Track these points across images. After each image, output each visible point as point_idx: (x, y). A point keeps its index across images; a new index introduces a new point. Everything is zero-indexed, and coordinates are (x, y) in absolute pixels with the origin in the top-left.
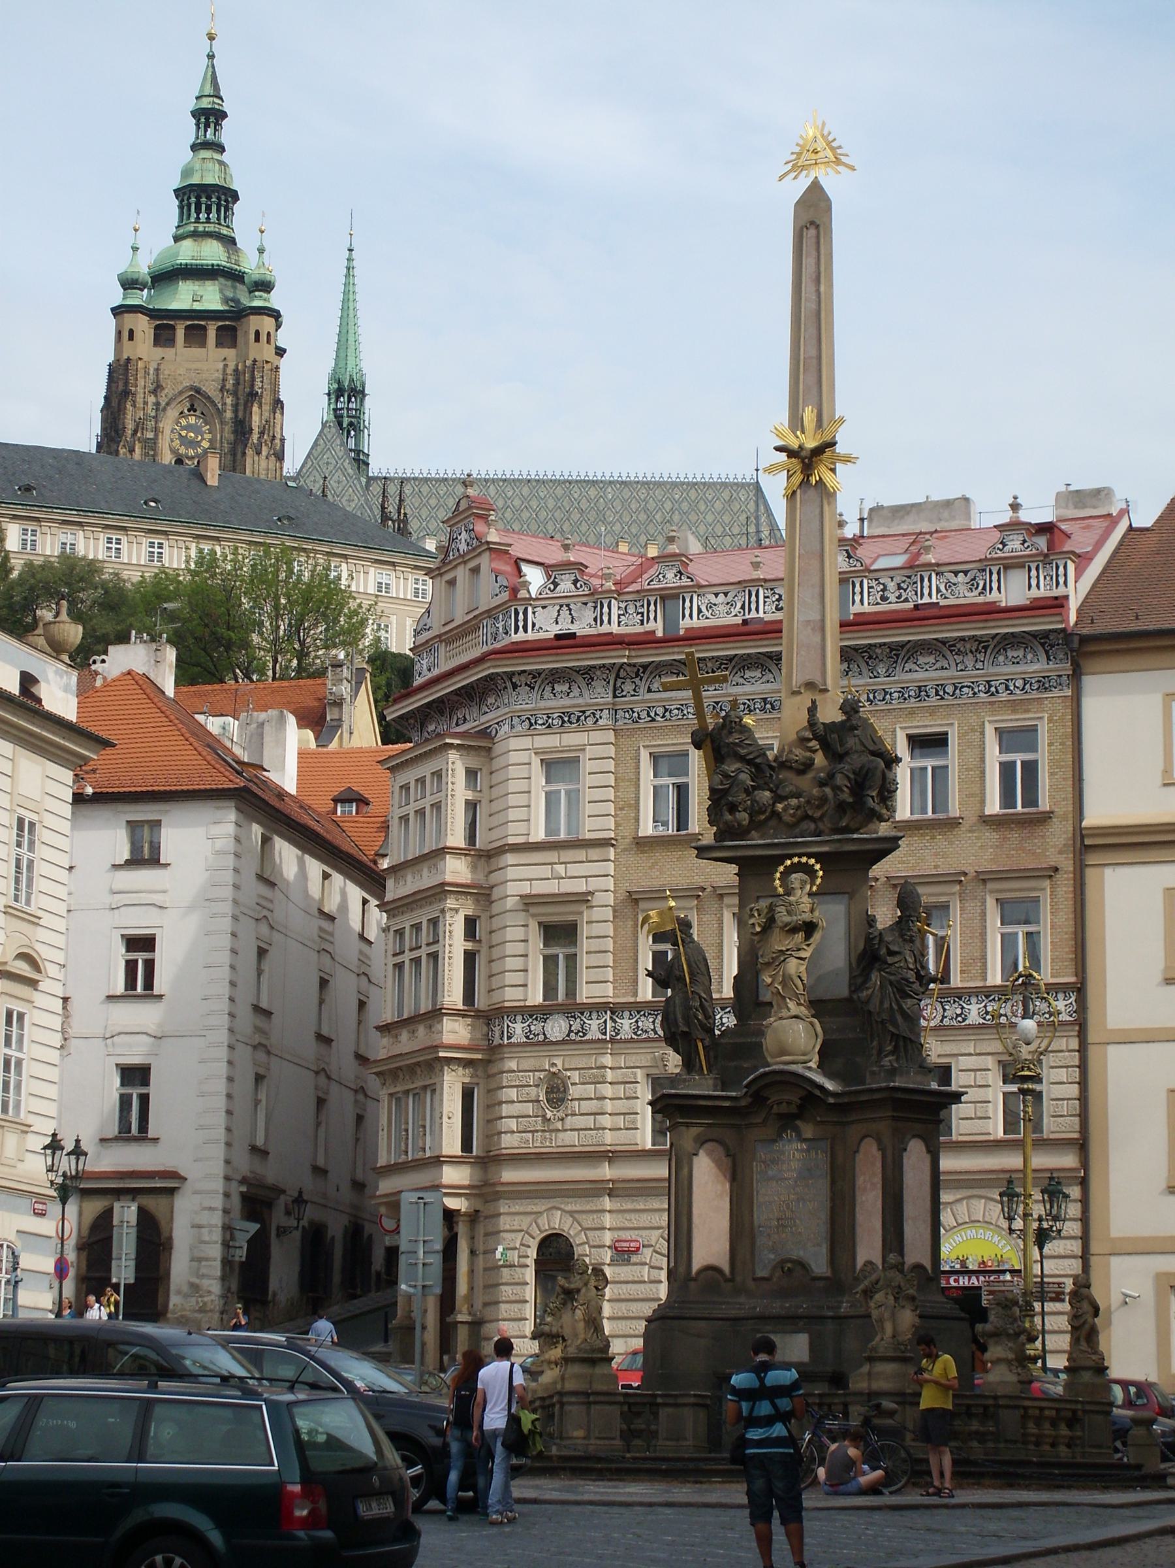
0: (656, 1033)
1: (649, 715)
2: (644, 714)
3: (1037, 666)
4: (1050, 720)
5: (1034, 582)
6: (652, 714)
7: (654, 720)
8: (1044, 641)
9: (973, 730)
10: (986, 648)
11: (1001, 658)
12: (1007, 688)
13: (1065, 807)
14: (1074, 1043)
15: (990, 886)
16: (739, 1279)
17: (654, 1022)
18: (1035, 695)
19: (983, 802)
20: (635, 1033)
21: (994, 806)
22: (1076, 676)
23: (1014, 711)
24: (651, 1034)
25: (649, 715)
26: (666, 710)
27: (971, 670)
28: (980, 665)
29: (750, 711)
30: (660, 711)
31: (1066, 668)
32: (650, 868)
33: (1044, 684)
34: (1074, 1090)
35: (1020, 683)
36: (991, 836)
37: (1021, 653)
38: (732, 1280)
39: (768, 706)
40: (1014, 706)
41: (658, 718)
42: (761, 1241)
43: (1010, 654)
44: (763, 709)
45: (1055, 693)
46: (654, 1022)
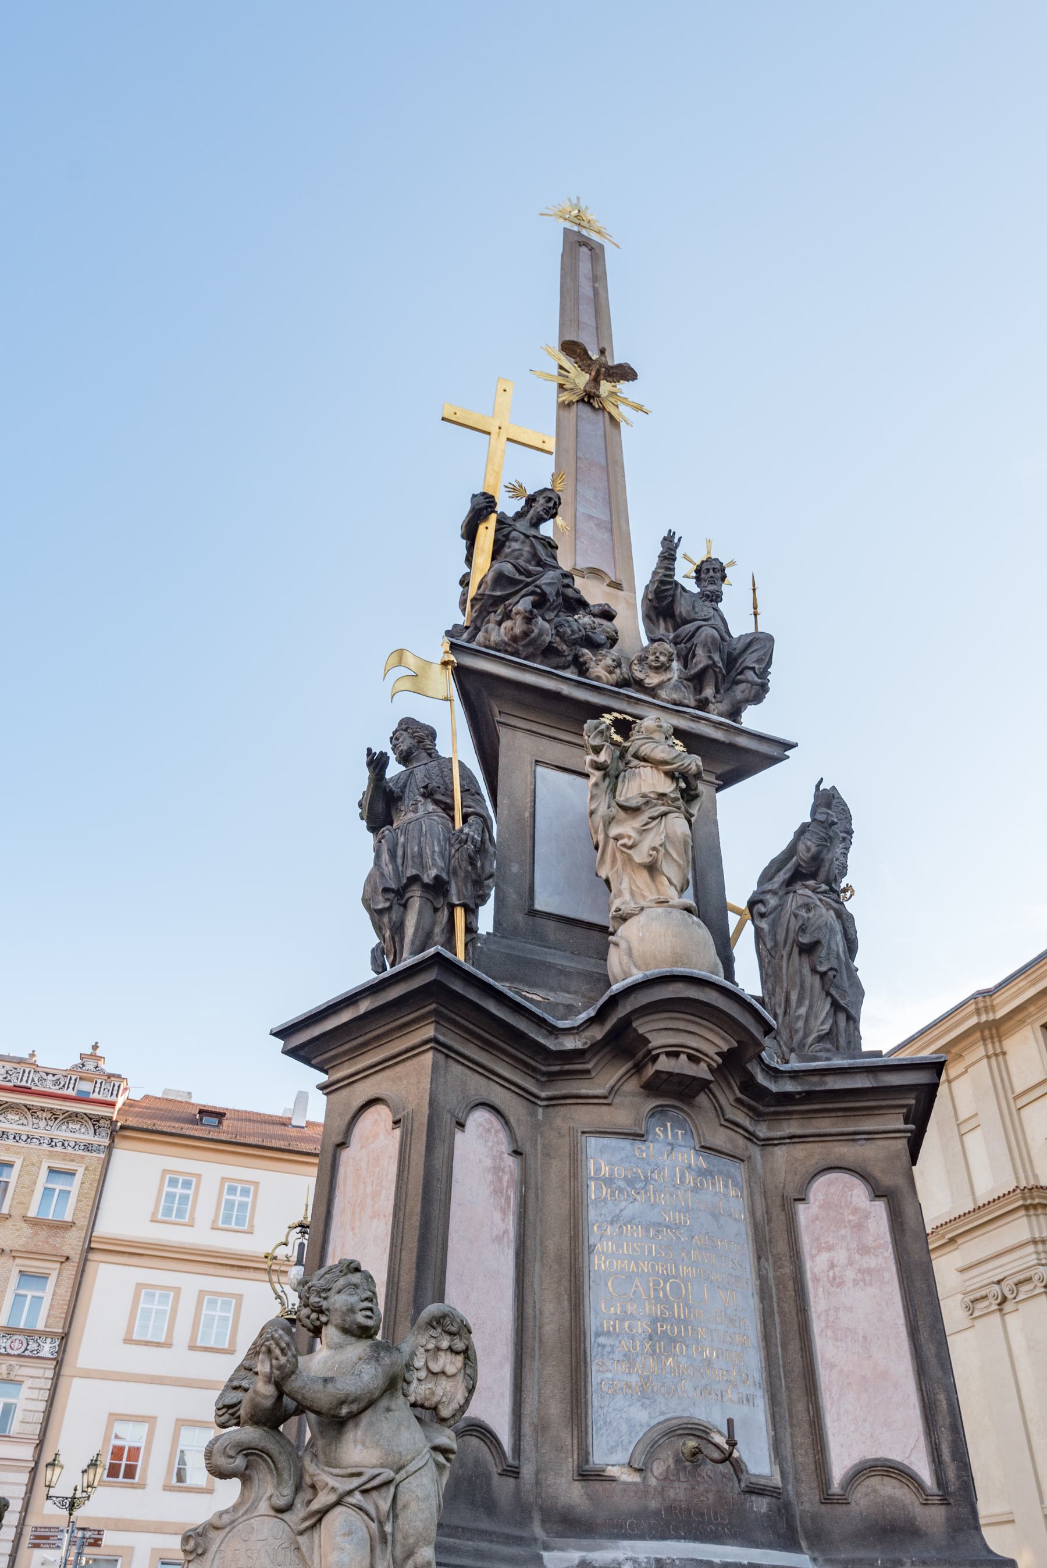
3: (86, 1135)
4: (86, 1169)
5: (97, 1090)
8: (95, 1121)
10: (56, 1119)
11: (64, 1127)
12: (63, 1145)
13: (83, 1222)
14: (50, 1374)
15: (18, 1261)
16: (527, 1471)
18: (81, 1152)
19: (28, 1208)
21: (32, 1213)
22: (110, 1148)
23: (64, 1159)
27: (42, 1129)
28: (48, 1128)
31: (106, 1142)
33: (88, 1148)
34: (42, 1406)
35: (72, 1144)
36: (27, 1230)
37: (78, 1127)
38: (513, 1472)
40: (65, 1157)
42: (605, 1373)
43: (71, 1125)
45: (94, 1154)
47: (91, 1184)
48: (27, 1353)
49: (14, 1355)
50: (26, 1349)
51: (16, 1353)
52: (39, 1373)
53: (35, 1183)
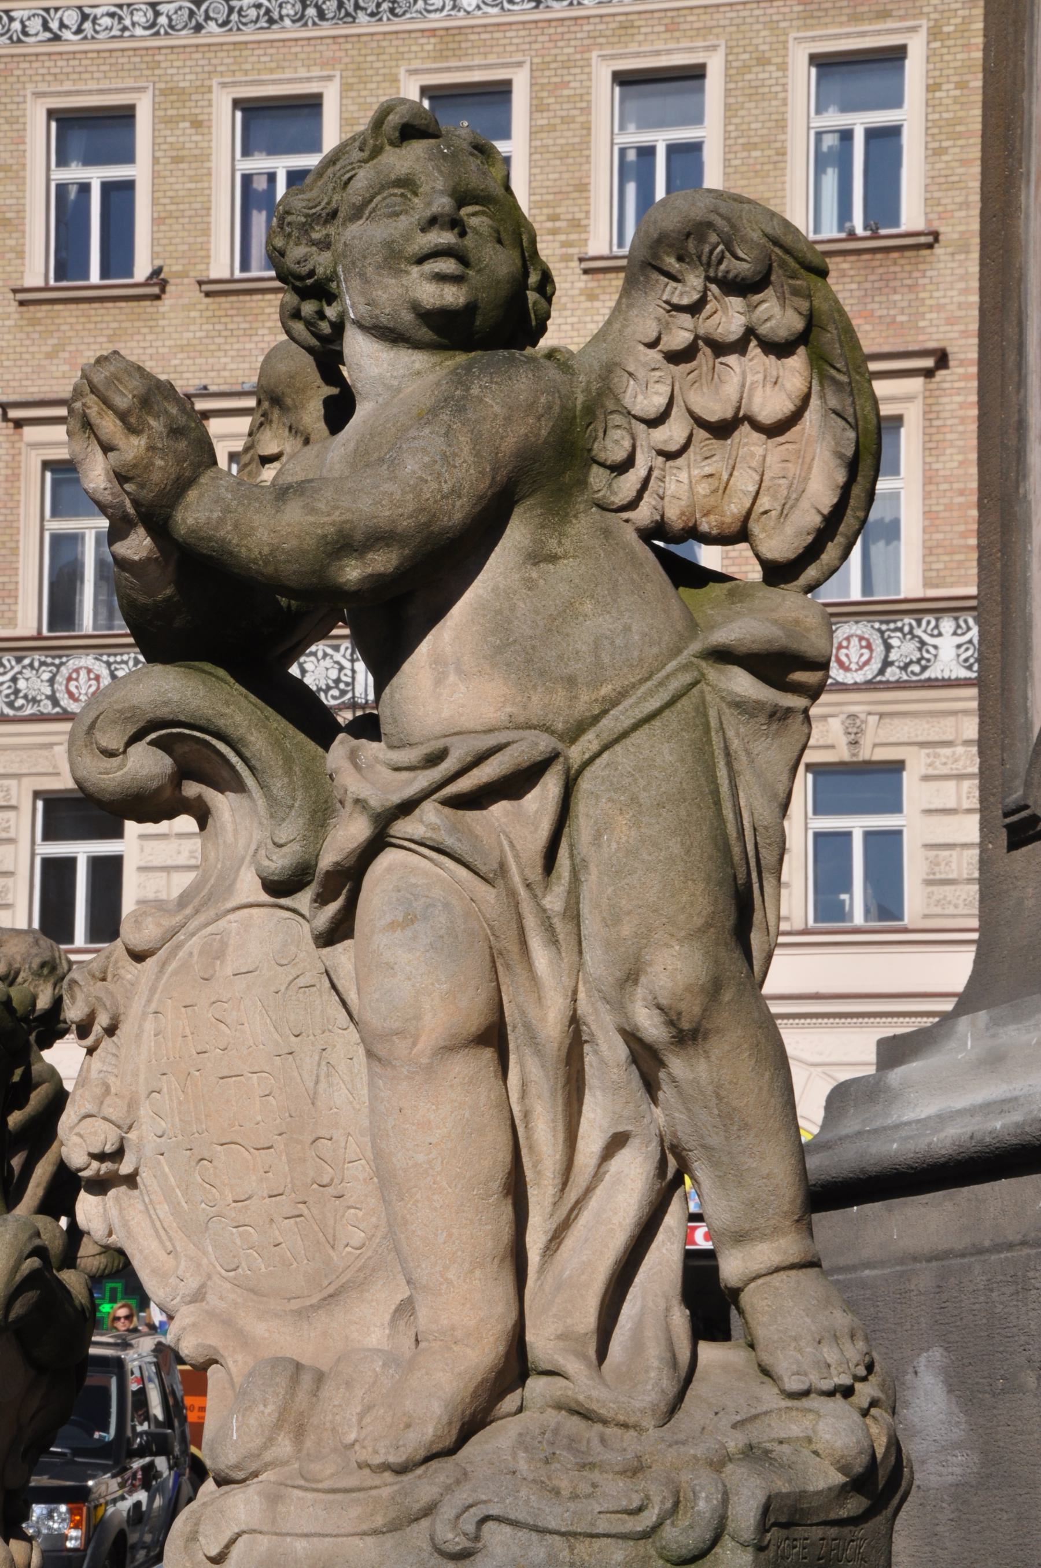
0: (55, 702)
1: (46, 27)
2: (35, 25)
4: (934, 34)
6: (54, 25)
7: (57, 38)
9: (763, 61)
17: (52, 681)
20: (11, 705)
24: (47, 707)
25: (46, 27)
26: (85, 17)
29: (271, 21)
30: (72, 18)
32: (49, 356)
39: (311, 12)
41: (67, 35)
44: (300, 19)
46: (52, 681)
47: (962, 85)
48: (892, 674)
49: (856, 687)
50: (886, 664)
51: (859, 677)
52: (945, 729)
53: (781, 125)
